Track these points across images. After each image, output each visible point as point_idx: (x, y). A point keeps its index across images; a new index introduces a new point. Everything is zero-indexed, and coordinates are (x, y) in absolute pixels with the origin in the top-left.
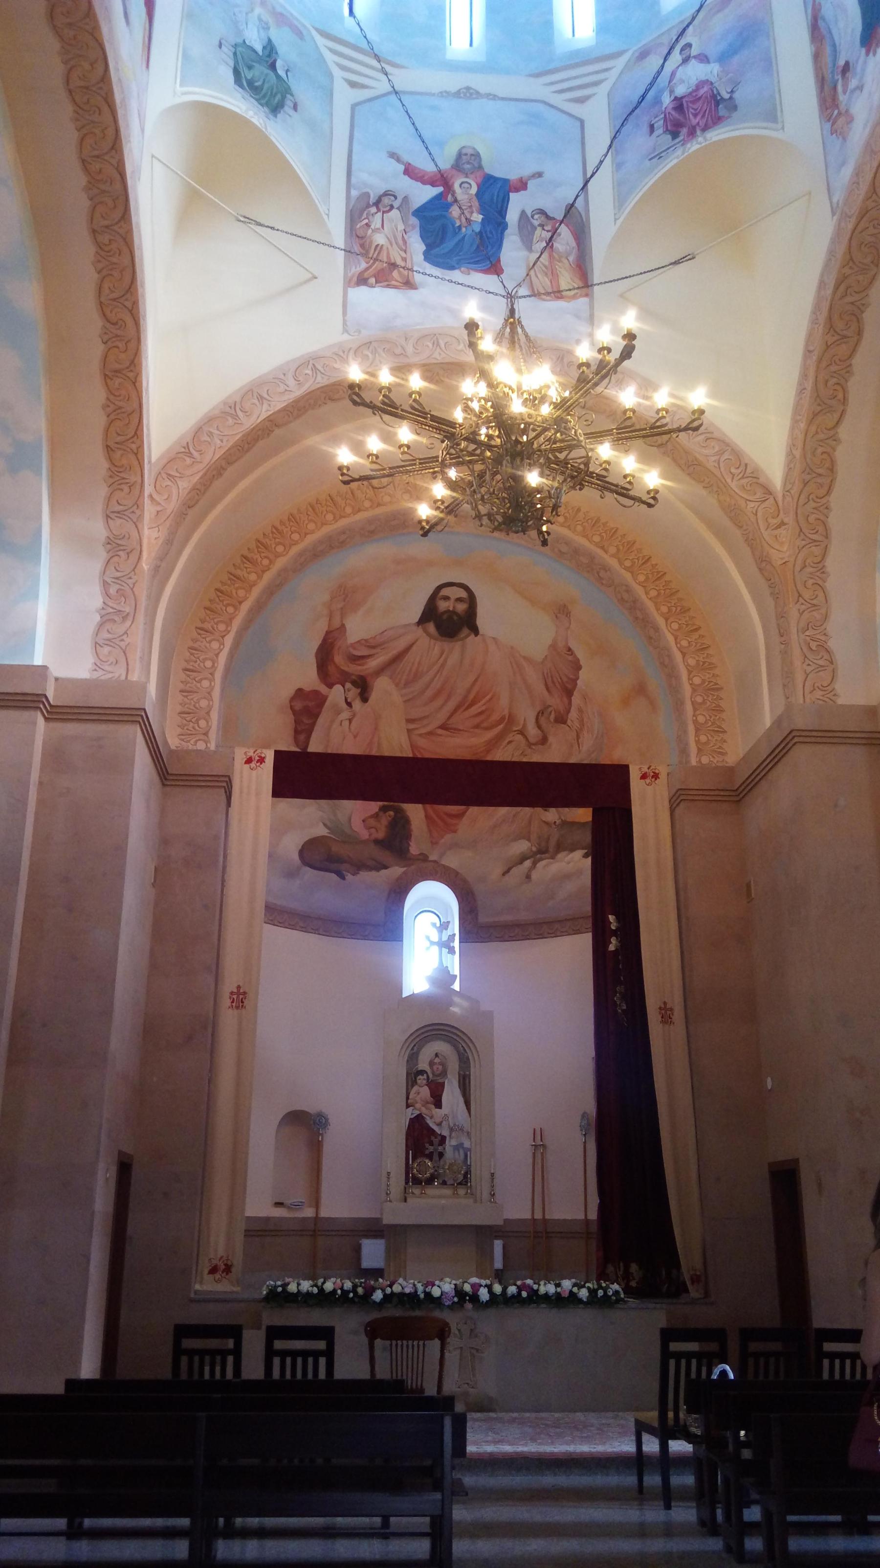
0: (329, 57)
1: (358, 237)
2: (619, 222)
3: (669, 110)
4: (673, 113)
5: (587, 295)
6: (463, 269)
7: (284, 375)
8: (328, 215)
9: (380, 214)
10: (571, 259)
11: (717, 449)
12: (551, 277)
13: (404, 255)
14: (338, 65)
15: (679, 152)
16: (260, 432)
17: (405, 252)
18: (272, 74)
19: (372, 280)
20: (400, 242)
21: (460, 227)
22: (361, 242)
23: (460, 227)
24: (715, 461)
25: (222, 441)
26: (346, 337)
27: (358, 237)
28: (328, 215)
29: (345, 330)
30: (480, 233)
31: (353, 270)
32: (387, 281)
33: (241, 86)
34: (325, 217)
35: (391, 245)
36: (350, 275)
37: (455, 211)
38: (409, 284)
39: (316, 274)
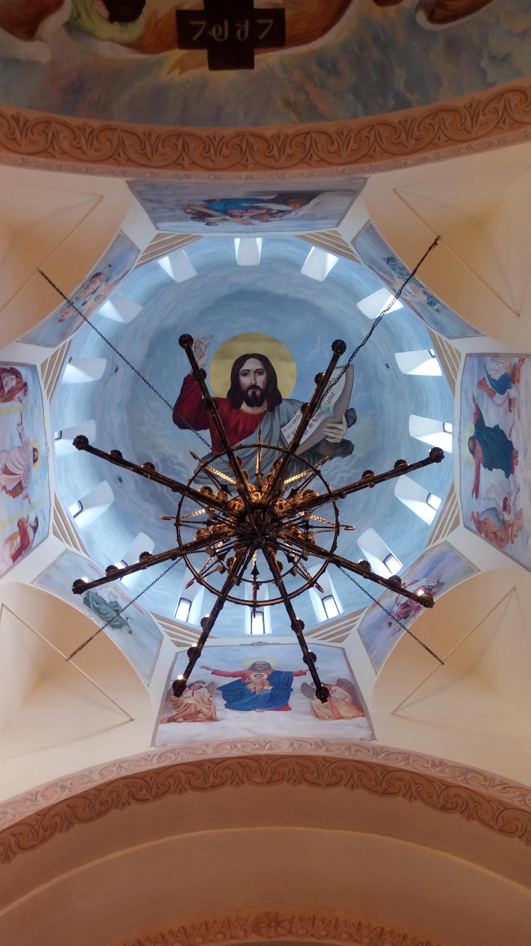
0: (160, 627)
1: (172, 701)
2: (379, 673)
3: (400, 610)
4: (402, 610)
5: (363, 716)
6: (257, 710)
7: (91, 773)
8: (148, 686)
9: (192, 691)
10: (347, 701)
11: (518, 793)
12: (331, 709)
13: (208, 706)
14: (165, 631)
15: (413, 620)
16: (57, 819)
17: (210, 705)
18: (115, 614)
19: (182, 719)
20: (206, 701)
21: (255, 693)
22: (174, 703)
23: (255, 693)
24: (520, 801)
25: (14, 816)
26: (153, 748)
27: (172, 701)
28: (148, 686)
29: (153, 744)
30: (271, 694)
31: (166, 716)
32: (193, 718)
33: (90, 607)
34: (146, 686)
35: (199, 702)
36: (162, 718)
37: (250, 687)
38: (212, 719)
39: (133, 717)
